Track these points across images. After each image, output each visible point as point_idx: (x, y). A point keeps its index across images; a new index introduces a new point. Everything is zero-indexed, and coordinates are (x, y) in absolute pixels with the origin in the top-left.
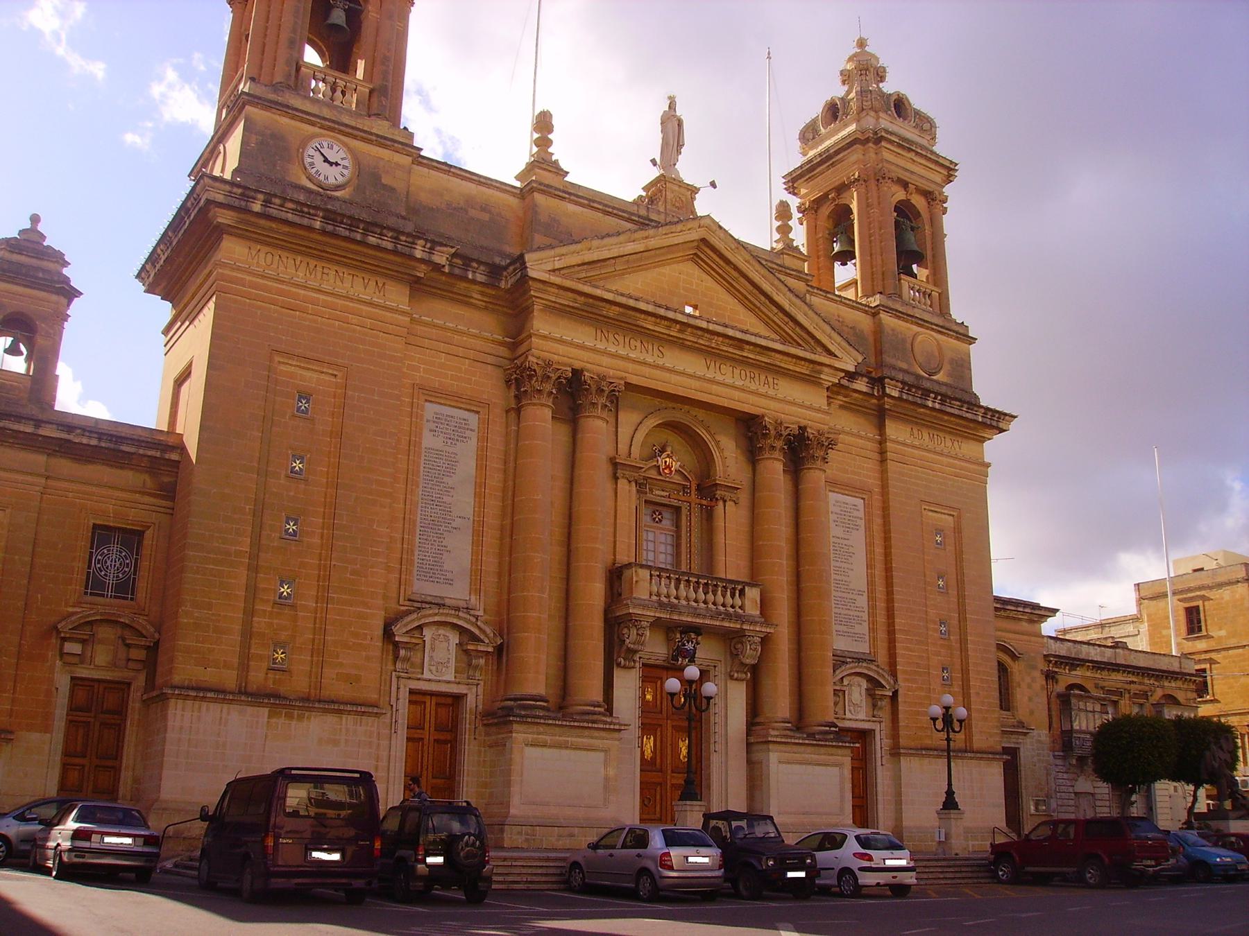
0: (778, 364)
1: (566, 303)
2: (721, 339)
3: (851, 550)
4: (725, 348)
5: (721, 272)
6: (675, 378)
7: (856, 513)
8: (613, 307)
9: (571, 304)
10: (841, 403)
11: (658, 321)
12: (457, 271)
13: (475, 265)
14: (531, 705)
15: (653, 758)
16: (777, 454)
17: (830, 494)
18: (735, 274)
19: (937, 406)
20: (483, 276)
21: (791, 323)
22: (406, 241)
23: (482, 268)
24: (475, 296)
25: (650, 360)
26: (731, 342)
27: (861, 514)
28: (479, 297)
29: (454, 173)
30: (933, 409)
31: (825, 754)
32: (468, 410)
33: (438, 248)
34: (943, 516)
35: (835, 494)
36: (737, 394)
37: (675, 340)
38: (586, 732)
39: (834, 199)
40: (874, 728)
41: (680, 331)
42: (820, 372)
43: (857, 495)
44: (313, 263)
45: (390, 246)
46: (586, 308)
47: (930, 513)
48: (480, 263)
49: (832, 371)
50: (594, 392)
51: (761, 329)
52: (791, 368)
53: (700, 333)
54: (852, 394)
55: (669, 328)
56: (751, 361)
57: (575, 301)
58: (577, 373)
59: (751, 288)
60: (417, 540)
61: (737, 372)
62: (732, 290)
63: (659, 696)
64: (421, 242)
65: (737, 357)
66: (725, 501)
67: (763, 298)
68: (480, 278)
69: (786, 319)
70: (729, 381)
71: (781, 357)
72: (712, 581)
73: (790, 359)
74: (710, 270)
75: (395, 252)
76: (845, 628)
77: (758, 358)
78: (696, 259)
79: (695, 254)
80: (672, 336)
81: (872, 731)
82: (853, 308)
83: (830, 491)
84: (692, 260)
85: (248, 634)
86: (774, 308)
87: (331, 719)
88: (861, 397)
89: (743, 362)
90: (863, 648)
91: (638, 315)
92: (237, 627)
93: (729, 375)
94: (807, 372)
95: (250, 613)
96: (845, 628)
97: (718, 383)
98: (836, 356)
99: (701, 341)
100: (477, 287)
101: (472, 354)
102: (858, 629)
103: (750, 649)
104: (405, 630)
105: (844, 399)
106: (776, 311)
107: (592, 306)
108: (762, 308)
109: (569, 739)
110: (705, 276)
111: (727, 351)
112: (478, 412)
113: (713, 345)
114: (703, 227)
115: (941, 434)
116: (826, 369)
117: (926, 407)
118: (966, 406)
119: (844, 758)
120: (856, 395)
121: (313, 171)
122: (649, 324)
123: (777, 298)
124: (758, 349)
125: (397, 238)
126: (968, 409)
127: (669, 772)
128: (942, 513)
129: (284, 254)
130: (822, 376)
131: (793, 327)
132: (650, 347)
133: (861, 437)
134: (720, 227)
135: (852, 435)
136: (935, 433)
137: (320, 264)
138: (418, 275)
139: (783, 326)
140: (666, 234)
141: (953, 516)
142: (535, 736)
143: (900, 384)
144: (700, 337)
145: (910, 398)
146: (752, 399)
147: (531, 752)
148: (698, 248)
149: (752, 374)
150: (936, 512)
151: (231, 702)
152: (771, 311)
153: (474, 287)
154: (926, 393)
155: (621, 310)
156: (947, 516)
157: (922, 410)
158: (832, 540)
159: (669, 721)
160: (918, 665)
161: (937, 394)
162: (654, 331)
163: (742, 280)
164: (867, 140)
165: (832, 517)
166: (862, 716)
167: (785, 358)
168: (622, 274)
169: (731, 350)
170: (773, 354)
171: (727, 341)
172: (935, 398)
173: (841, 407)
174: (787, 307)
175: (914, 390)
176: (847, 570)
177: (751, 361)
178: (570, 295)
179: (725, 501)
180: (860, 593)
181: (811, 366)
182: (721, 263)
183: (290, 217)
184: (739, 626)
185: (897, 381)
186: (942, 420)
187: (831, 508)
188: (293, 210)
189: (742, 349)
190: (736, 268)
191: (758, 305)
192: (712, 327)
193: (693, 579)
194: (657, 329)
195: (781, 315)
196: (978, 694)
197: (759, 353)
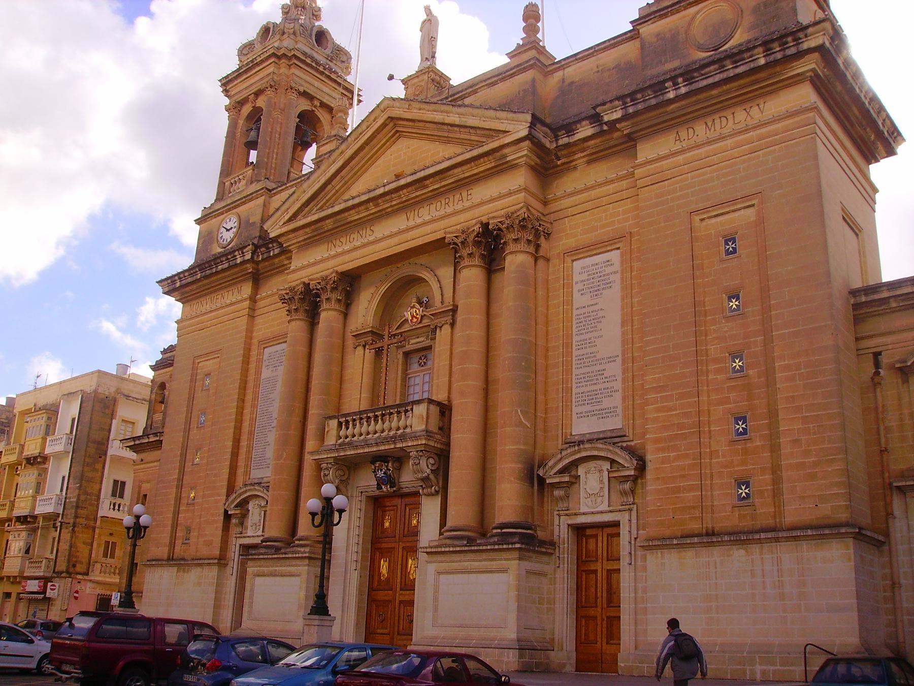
0: (462, 176)
1: (302, 239)
2: (405, 191)
3: (600, 314)
4: (414, 195)
7: (609, 270)
9: (306, 237)
10: (585, 159)
11: (357, 210)
14: (270, 545)
15: (388, 579)
16: (477, 261)
19: (683, 90)
20: (279, 249)
21: (472, 131)
22: (232, 257)
25: (358, 244)
26: (413, 188)
27: (617, 266)
29: (290, 186)
30: (678, 98)
31: (485, 560)
32: (279, 344)
33: (245, 251)
34: (737, 214)
35: (581, 261)
37: (379, 214)
38: (288, 562)
40: (617, 519)
41: (377, 205)
42: (505, 156)
43: (609, 248)
45: (226, 266)
47: (713, 221)
49: (513, 148)
50: (329, 290)
51: (458, 149)
52: (475, 172)
54: (586, 144)
56: (442, 190)
57: (307, 233)
60: (255, 443)
61: (433, 207)
62: (431, 138)
64: (236, 253)
65: (429, 194)
69: (467, 130)
70: (427, 218)
71: (459, 170)
72: (385, 411)
74: (410, 136)
75: (230, 268)
76: (588, 408)
77: (444, 183)
78: (398, 135)
80: (373, 214)
81: (616, 524)
82: (613, 46)
85: (175, 525)
87: (199, 569)
88: (598, 141)
89: (436, 195)
90: (614, 423)
91: (343, 215)
92: (170, 522)
93: (426, 213)
94: (493, 164)
95: (176, 513)
96: (588, 408)
97: (412, 228)
99: (394, 203)
102: (607, 403)
104: (233, 506)
105: (582, 155)
107: (317, 230)
109: (277, 568)
111: (417, 197)
113: (404, 199)
114: (385, 110)
115: (728, 113)
117: (671, 101)
118: (727, 62)
119: (509, 562)
120: (592, 143)
122: (354, 216)
123: (448, 120)
124: (437, 178)
125: (228, 259)
126: (735, 62)
127: (398, 589)
128: (734, 211)
130: (508, 159)
133: (612, 181)
134: (393, 99)
135: (601, 185)
136: (716, 117)
138: (250, 271)
141: (753, 205)
142: (259, 568)
143: (617, 103)
144: (391, 200)
145: (640, 107)
147: (259, 580)
150: (722, 214)
151: (162, 565)
152: (455, 132)
154: (658, 87)
155: (332, 220)
156: (742, 212)
157: (672, 106)
160: (681, 426)
161: (673, 79)
162: (360, 219)
163: (428, 125)
165: (576, 288)
166: (604, 507)
167: (464, 168)
168: (347, 185)
170: (451, 172)
171: (410, 189)
172: (676, 84)
173: (589, 162)
175: (639, 96)
176: (593, 340)
177: (442, 190)
178: (301, 232)
180: (611, 359)
181: (491, 157)
183: (190, 280)
184: (392, 446)
185: (611, 101)
186: (712, 98)
188: (189, 275)
189: (426, 186)
190: (419, 121)
192: (387, 188)
193: (343, 420)
194: (361, 216)
196: (796, 442)
197: (441, 180)
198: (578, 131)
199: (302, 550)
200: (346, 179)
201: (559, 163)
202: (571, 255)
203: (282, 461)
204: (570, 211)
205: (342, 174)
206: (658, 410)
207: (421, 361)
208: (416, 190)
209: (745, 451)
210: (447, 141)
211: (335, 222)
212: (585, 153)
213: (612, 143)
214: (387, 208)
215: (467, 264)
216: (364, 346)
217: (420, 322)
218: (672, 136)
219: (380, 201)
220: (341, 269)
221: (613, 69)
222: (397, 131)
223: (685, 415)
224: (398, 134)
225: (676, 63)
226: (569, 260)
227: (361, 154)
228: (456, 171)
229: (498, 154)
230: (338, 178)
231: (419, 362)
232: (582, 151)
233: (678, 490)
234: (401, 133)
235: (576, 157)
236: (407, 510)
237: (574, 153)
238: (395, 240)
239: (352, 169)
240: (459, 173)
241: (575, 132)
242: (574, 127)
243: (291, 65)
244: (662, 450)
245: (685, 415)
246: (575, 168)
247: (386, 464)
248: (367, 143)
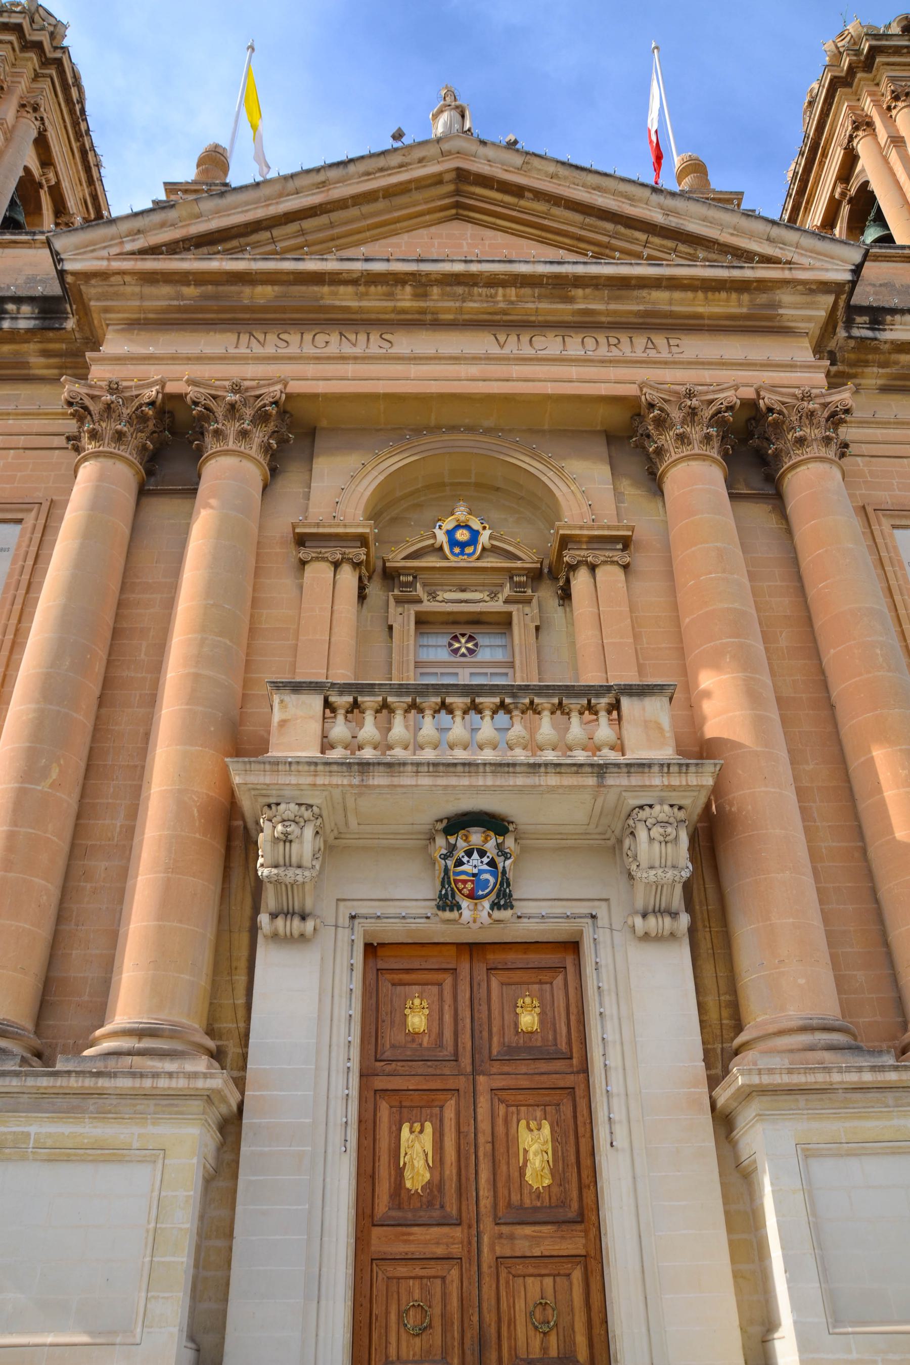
2: (512, 292)
5: (514, 213)
6: (414, 370)
8: (259, 289)
11: (362, 289)
13: (10, 307)
15: (435, 1188)
17: (897, 532)
18: (541, 207)
23: (26, 309)
28: (42, 360)
36: (574, 371)
39: (843, 194)
46: (209, 303)
48: (18, 300)
53: (460, 290)
55: (390, 296)
59: (578, 217)
63: (448, 1018)
66: (593, 568)
67: (609, 226)
68: (23, 324)
72: (514, 696)
73: (690, 295)
79: (457, 205)
83: (894, 527)
84: (457, 217)
100: (32, 347)
101: (22, 441)
103: (651, 840)
106: (642, 236)
107: (216, 297)
108: (613, 241)
110: (489, 233)
112: (19, 521)
131: (691, 251)
140: (368, 174)
146: (613, 372)
148: (457, 193)
149: (613, 341)
153: (25, 347)
155: (276, 288)
159: (481, 1079)
162: (360, 310)
164: (852, 71)
169: (544, 305)
170: (644, 293)
171: (527, 291)
173: (884, 390)
174: (657, 217)
179: (593, 568)
182: (508, 199)
189: (571, 300)
190: (539, 195)
191: (605, 239)
194: (364, 304)
195: (656, 240)
198: (891, 327)
199: (170, 1066)
200: (336, 231)
202: (892, 516)
203: (43, 787)
204: (865, 449)
205: (307, 224)
207: (463, 640)
208: (540, 298)
212: (888, 370)
214: (448, 310)
215: (674, 457)
216: (336, 565)
217: (478, 559)
219: (435, 290)
221: (881, 285)
224: (454, 211)
226: (886, 523)
227: (366, 209)
229: (762, 298)
230: (293, 227)
231: (450, 645)
234: (461, 212)
235: (868, 370)
236: (494, 984)
238: (474, 370)
239: (332, 225)
240: (660, 299)
241: (886, 327)
242: (889, 318)
243: (44, 76)
247: (500, 839)
248: (389, 193)
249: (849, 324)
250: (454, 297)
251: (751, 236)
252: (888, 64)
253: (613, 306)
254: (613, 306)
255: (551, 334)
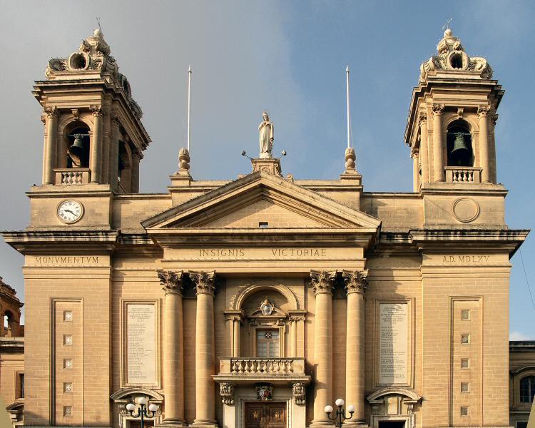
6: (250, 264)
12: (127, 243)
24: (144, 252)
41: (249, 239)
44: (64, 257)
53: (262, 237)
58: (185, 276)
69: (326, 214)
86: (317, 210)
88: (401, 247)
98: (360, 226)
106: (318, 211)
116: (357, 237)
121: (67, 219)
129: (51, 257)
132: (235, 252)
137: (67, 257)
139: (325, 218)
146: (305, 264)
158: (381, 329)
160: (440, 385)
165: (381, 317)
170: (314, 236)
173: (391, 256)
187: (382, 312)
191: (307, 211)
195: (322, 212)
201: (375, 251)
206: (429, 378)
209: (467, 397)
210: (306, 215)
211: (210, 239)
213: (408, 250)
218: (442, 257)
220: (219, 271)
222: (263, 195)
223: (442, 381)
225: (443, 221)
228: (319, 237)
229: (350, 237)
232: (390, 249)
233: (438, 410)
237: (386, 249)
244: (431, 393)
245: (442, 381)
246: (382, 257)
249: (380, 238)
250: (260, 239)
251: (350, 214)
252: (435, 90)
253: (306, 241)
254: (306, 241)
255: (289, 249)
